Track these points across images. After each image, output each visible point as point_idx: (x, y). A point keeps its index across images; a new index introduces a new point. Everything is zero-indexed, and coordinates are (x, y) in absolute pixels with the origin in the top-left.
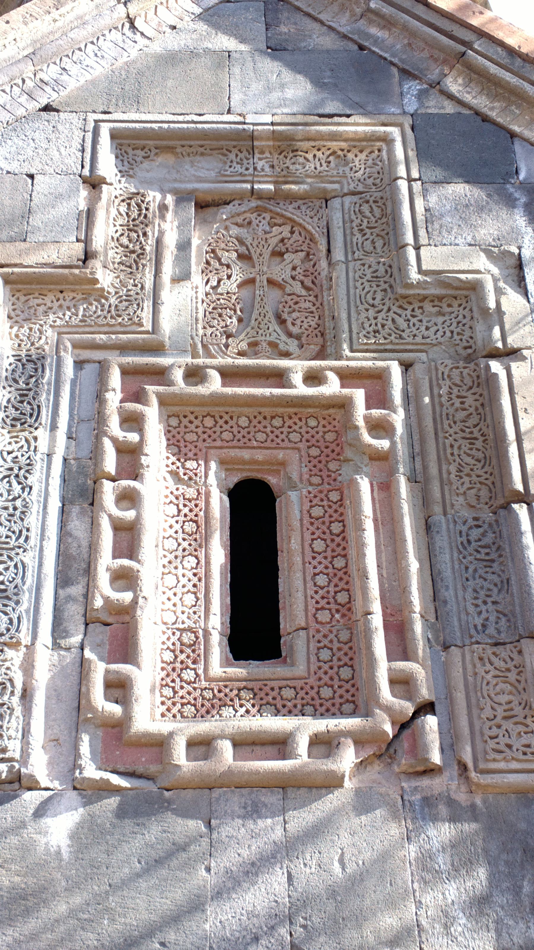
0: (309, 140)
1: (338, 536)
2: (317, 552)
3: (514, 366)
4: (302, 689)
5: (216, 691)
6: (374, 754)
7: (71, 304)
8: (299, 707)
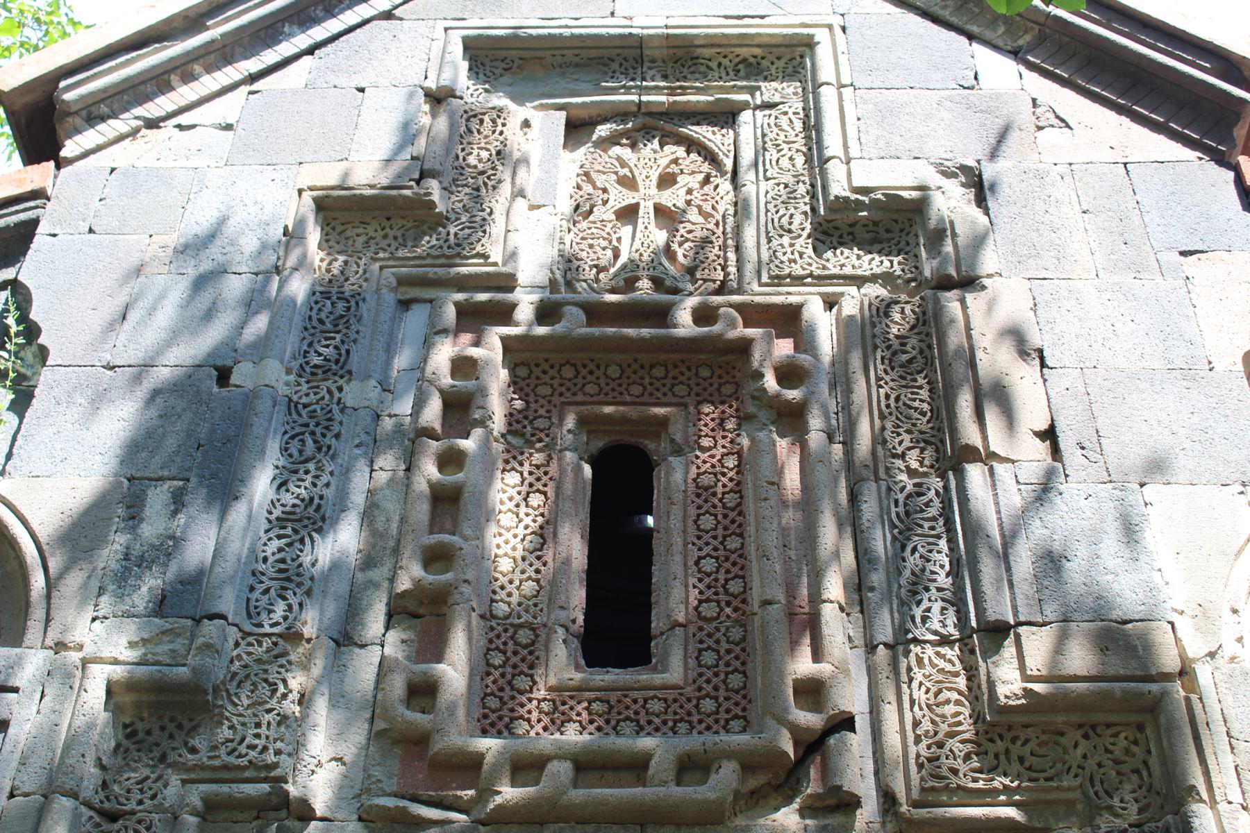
0: (712, 46)
1: (733, 509)
2: (703, 531)
3: (969, 298)
4: (675, 701)
5: (558, 703)
6: (769, 783)
7: (399, 234)
8: (670, 724)
